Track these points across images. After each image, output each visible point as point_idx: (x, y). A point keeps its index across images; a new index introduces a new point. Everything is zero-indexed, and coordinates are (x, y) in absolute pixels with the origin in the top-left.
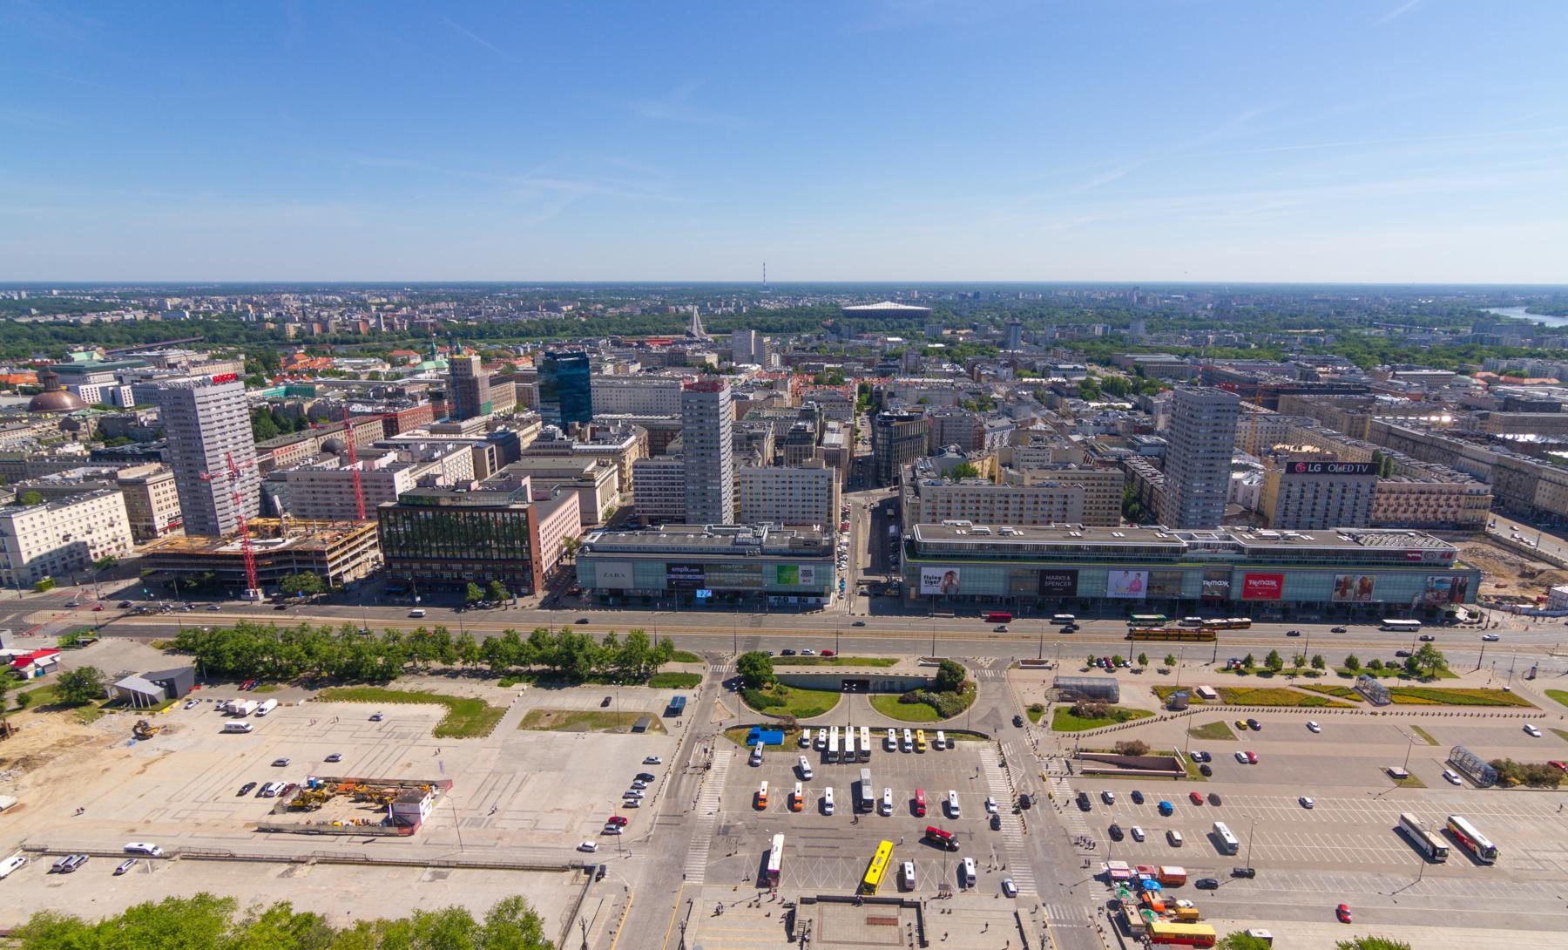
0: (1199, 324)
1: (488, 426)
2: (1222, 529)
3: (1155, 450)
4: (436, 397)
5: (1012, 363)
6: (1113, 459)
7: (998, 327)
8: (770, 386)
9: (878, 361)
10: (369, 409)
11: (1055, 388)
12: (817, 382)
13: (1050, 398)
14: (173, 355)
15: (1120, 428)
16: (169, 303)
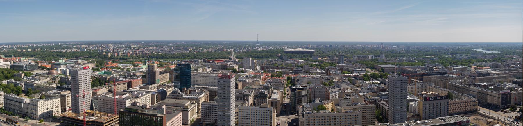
0: (401, 55)
1: (158, 88)
2: (406, 122)
3: (386, 97)
4: (143, 77)
5: (341, 69)
6: (373, 101)
7: (337, 57)
8: (255, 77)
9: (295, 68)
10: (124, 80)
11: (355, 77)
12: (272, 76)
13: (353, 81)
14: (80, 61)
15: (375, 90)
16: (82, 46)
